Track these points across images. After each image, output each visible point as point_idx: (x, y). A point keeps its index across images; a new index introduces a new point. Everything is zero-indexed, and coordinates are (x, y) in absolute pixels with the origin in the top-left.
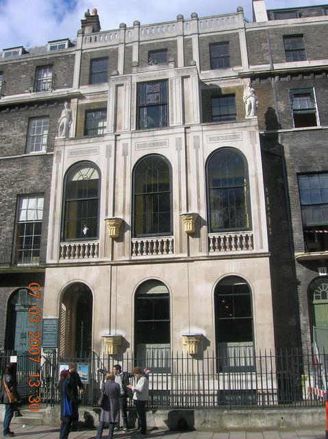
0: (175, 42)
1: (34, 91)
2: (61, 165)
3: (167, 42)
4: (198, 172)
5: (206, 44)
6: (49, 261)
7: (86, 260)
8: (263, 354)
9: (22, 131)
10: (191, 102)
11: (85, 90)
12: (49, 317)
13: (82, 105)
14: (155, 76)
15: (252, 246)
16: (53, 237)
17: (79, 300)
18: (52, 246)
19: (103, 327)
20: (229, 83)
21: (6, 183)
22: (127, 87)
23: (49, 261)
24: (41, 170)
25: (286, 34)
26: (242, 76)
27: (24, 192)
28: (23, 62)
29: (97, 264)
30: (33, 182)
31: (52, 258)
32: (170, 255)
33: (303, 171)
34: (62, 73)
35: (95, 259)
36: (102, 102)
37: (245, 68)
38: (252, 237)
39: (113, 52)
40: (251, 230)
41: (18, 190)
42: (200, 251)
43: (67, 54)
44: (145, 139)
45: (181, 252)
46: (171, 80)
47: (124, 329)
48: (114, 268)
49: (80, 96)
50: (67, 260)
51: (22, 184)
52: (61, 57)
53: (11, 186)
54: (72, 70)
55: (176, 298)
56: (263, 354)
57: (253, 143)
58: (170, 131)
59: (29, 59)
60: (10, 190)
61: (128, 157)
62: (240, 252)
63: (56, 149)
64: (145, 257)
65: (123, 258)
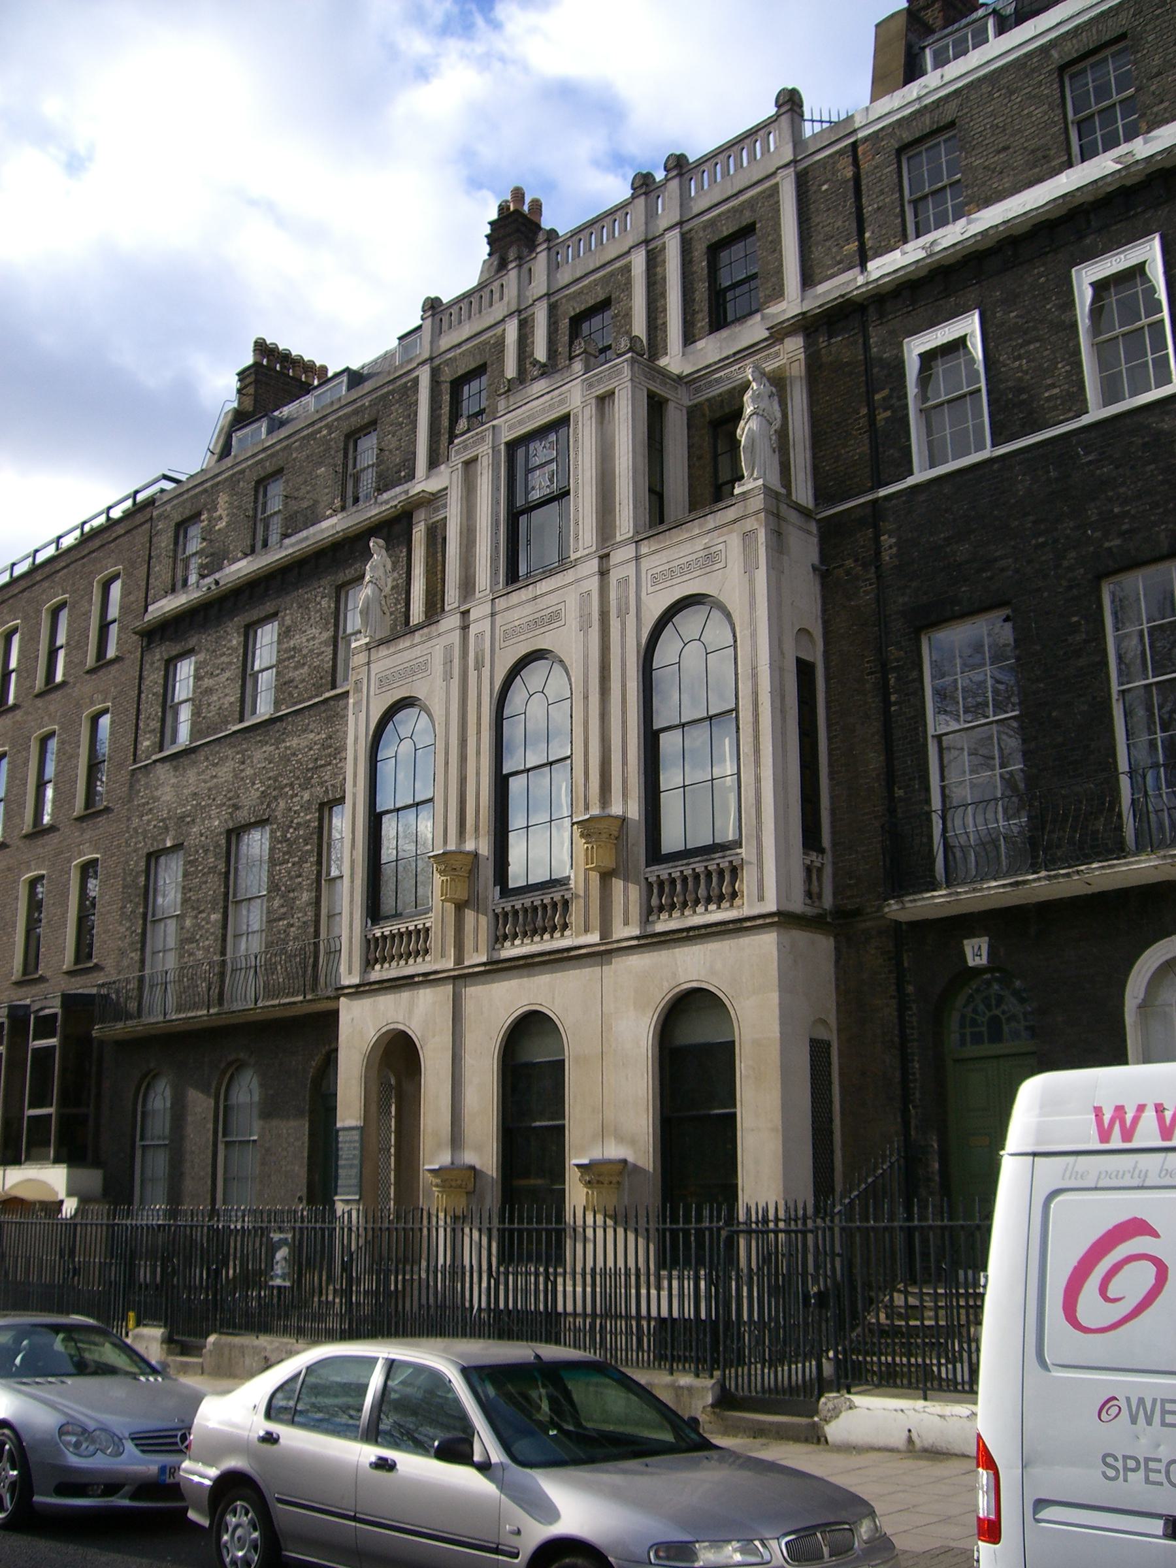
1: (343, 508)
14: (543, 411)
21: (298, 778)
27: (331, 796)
43: (404, 380)
46: (576, 415)
52: (391, 393)
54: (414, 423)
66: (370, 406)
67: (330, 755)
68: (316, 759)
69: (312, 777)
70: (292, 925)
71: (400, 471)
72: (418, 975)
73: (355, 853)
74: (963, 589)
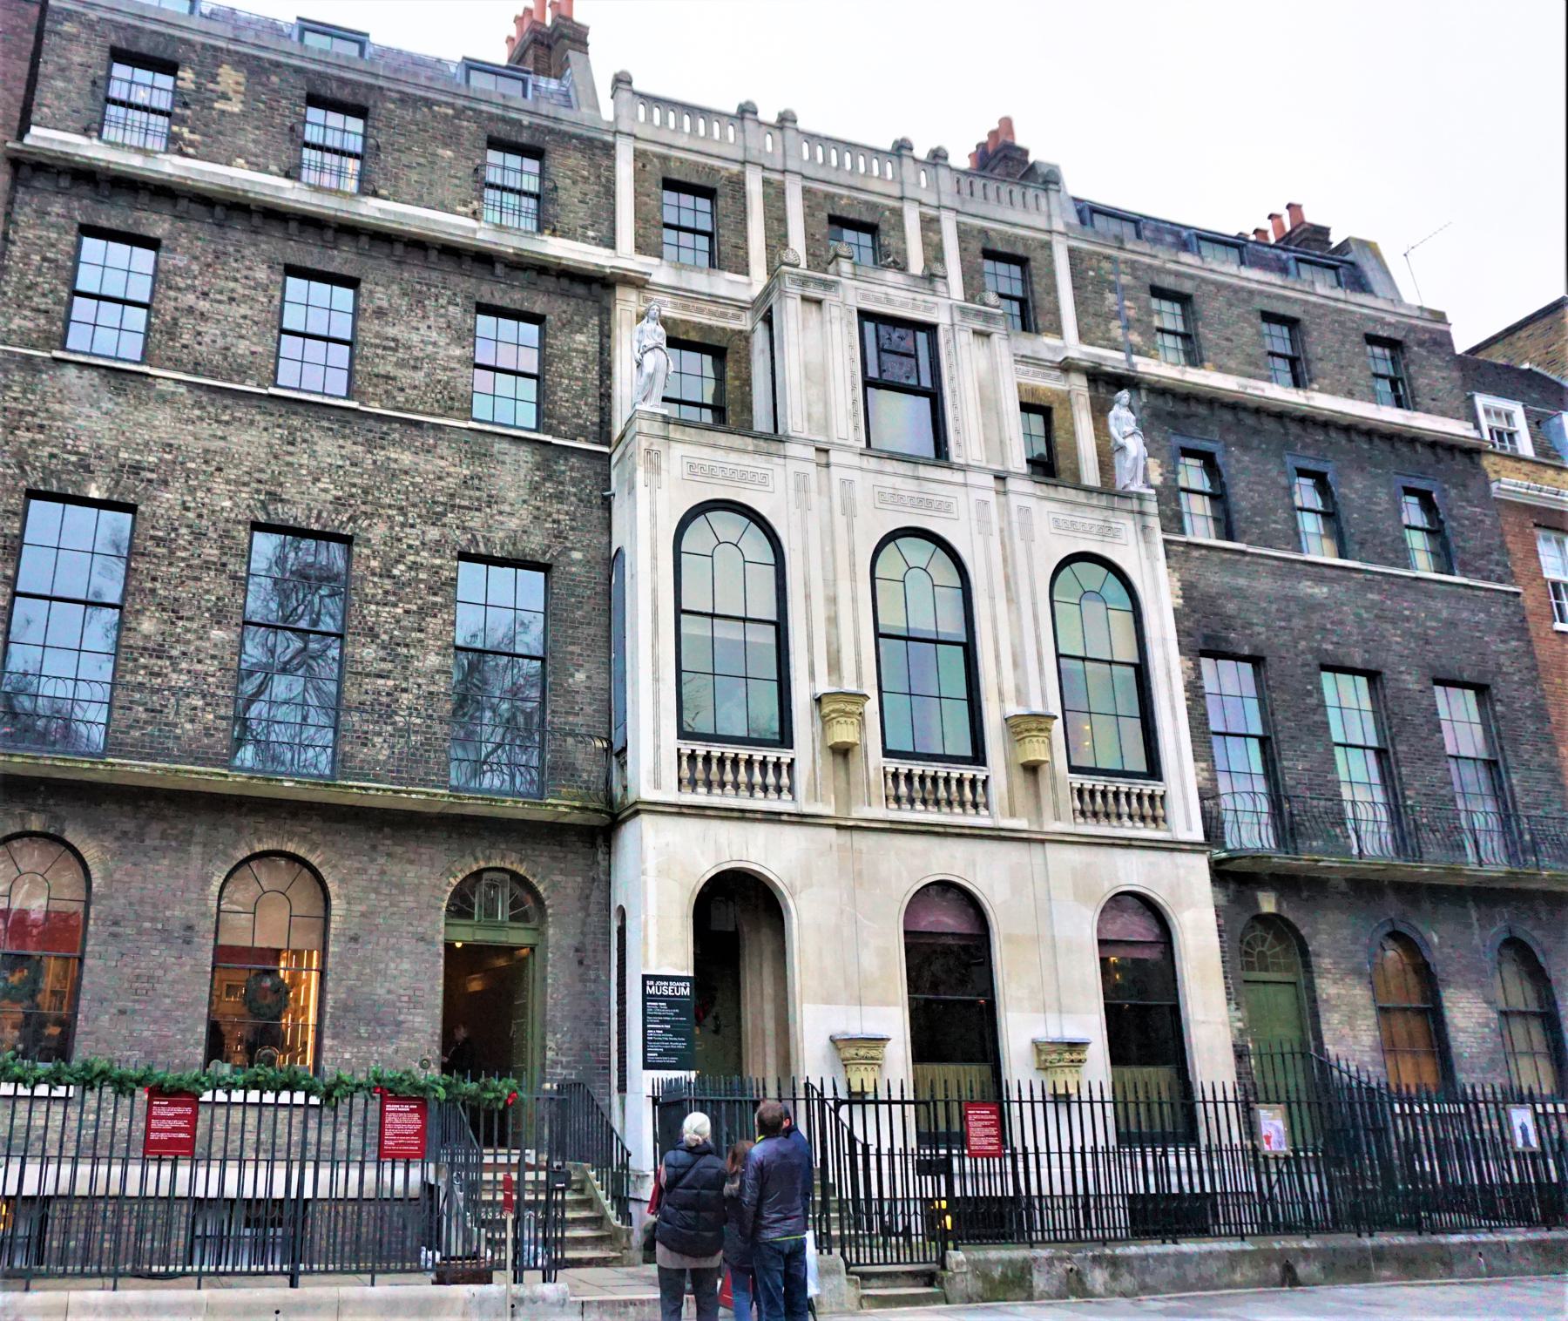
5: (976, 247)
20: (1035, 375)
21: (414, 505)
24: (535, 488)
26: (1067, 367)
27: (482, 550)
30: (513, 523)
34: (576, 192)
36: (710, 327)
37: (1072, 345)
39: (730, 180)
49: (638, 283)
51: (475, 521)
53: (435, 519)
54: (610, 192)
60: (433, 533)
67: (478, 499)
68: (452, 496)
70: (405, 690)
71: (586, 228)
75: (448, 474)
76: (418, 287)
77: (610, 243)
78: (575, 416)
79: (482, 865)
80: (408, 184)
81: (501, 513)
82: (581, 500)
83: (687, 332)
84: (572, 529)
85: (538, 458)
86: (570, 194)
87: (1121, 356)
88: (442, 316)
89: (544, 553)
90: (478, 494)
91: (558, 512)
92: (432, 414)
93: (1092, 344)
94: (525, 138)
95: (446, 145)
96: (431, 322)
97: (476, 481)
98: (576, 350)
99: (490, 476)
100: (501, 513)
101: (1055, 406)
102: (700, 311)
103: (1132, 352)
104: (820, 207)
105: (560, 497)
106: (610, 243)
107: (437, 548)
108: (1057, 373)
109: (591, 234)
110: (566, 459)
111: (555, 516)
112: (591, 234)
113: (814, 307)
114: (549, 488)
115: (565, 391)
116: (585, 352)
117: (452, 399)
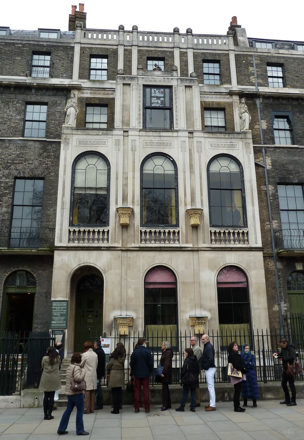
0: (172, 53)
2: (69, 152)
3: (164, 51)
4: (201, 173)
5: (200, 59)
6: (57, 244)
7: (96, 244)
8: (260, 334)
9: (19, 113)
10: (194, 110)
11: (85, 84)
12: (57, 299)
13: (83, 98)
14: (160, 81)
15: (248, 241)
16: (62, 220)
17: (88, 284)
18: (61, 230)
19: (114, 309)
20: (220, 98)
22: (134, 87)
23: (57, 244)
24: (40, 155)
25: (270, 61)
26: (231, 93)
27: (22, 175)
28: (17, 44)
29: (109, 249)
31: (61, 241)
32: (177, 245)
33: (283, 181)
34: (60, 63)
35: (105, 244)
37: (235, 86)
38: (247, 233)
40: (247, 227)
41: (15, 173)
42: (204, 242)
44: (152, 138)
45: (187, 242)
47: (135, 311)
48: (124, 254)
49: (79, 88)
50: (76, 244)
51: (20, 167)
54: (72, 61)
55: (183, 283)
56: (260, 334)
57: (248, 153)
58: (175, 134)
59: (24, 42)
60: (7, 172)
61: (137, 153)
62: (238, 245)
63: (64, 136)
64: (153, 245)
65: (133, 245)
66: (46, 46)
67: (22, 160)
68: (13, 160)
69: (10, 166)
72: (104, 247)
73: (64, 199)
74: (291, 176)
75: (13, 154)
76: (7, 100)
77: (71, 77)
78: (55, 131)
79: (16, 269)
80: (6, 69)
81: (29, 164)
82: (55, 157)
83: (95, 101)
84: (52, 166)
85: (42, 146)
86: (58, 64)
87: (254, 87)
88: (14, 107)
89: (42, 174)
90: (21, 159)
91: (47, 161)
92: (10, 137)
93: (243, 85)
94: (44, 50)
95: (19, 56)
96: (11, 109)
97: (21, 155)
98: (57, 112)
99: (26, 153)
100: (29, 164)
101: (227, 107)
102: (99, 94)
103: (258, 86)
104: (144, 55)
105: (48, 157)
106: (71, 77)
107: (7, 177)
108: (228, 96)
109: (64, 75)
110: (51, 145)
111: (46, 163)
112: (64, 75)
113: (128, 87)
114: (45, 154)
115: (53, 124)
116: (61, 112)
117: (16, 131)
